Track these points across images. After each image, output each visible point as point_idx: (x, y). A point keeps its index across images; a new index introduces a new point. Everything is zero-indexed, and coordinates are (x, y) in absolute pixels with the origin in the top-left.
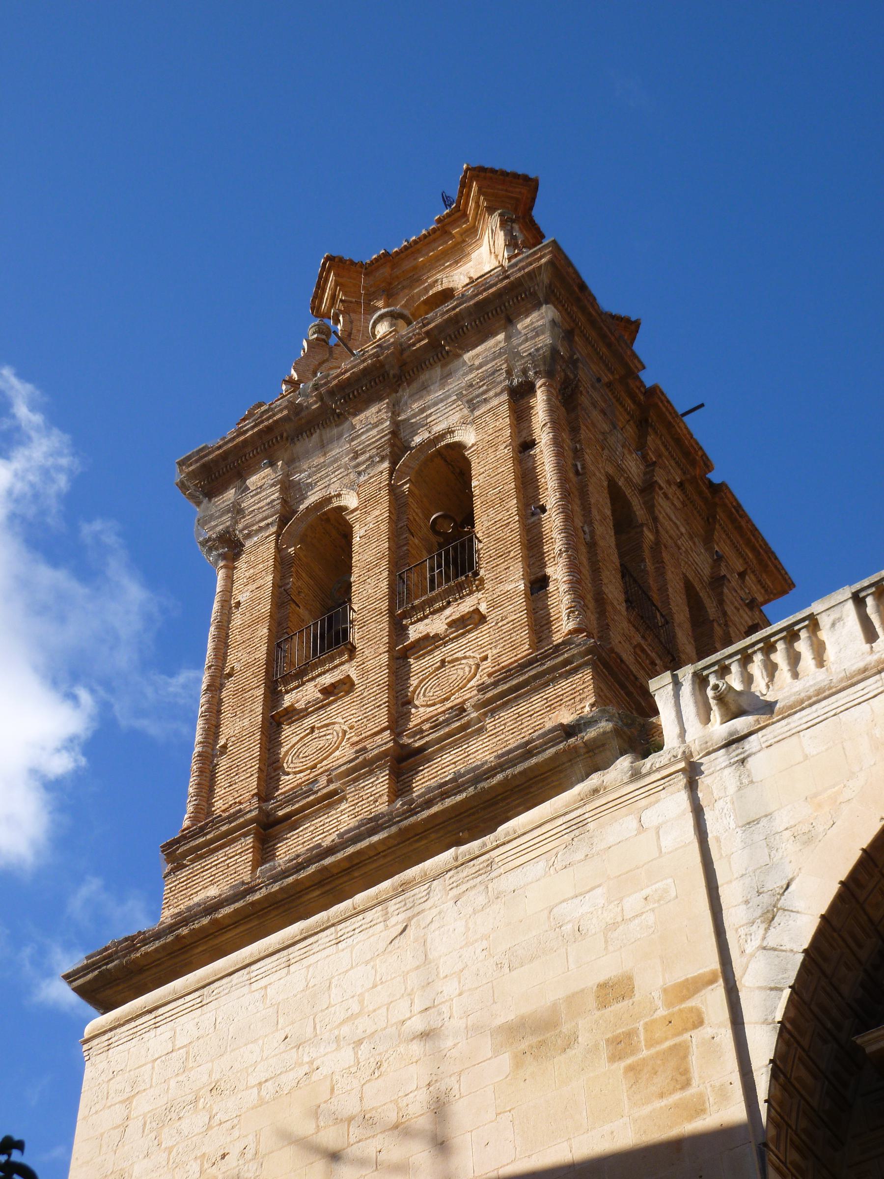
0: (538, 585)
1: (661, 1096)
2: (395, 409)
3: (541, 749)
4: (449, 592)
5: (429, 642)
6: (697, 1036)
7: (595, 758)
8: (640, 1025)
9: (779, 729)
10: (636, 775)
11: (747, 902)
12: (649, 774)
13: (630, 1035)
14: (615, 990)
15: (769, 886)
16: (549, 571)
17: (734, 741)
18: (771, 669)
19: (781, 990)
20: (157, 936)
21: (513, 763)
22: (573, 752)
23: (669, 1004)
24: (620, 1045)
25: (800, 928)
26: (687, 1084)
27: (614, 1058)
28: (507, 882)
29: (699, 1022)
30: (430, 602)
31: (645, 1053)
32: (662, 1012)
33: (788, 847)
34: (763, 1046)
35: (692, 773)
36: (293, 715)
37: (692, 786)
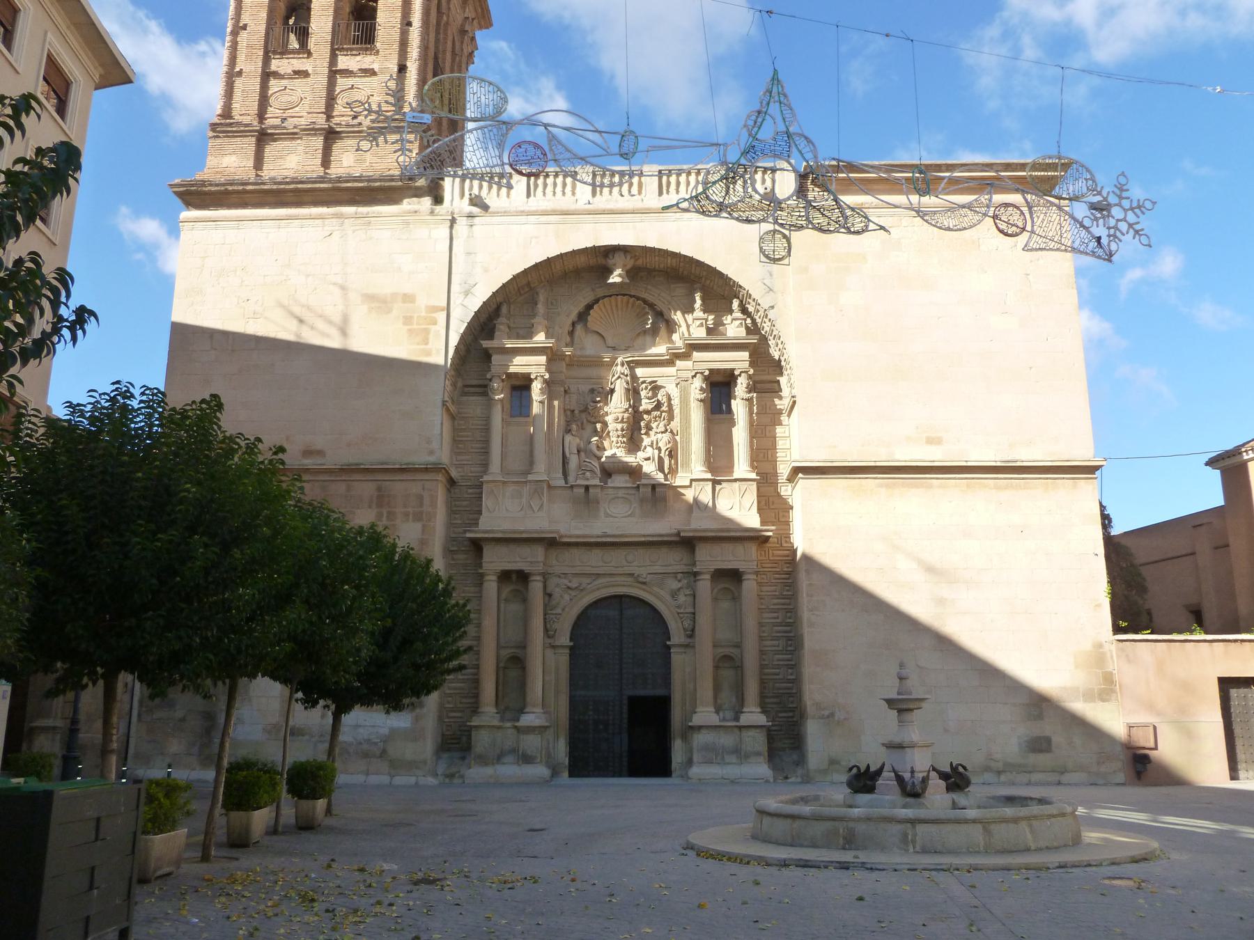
0: (402, 69)
4: (361, 49)
5: (347, 73)
6: (433, 328)
7: (418, 193)
9: (487, 219)
10: (432, 212)
13: (411, 317)
14: (408, 298)
16: (409, 64)
20: (217, 185)
24: (408, 320)
25: (475, 303)
26: (427, 344)
27: (405, 324)
29: (435, 323)
30: (351, 50)
31: (415, 327)
32: (423, 314)
34: (454, 340)
35: (453, 221)
36: (276, 75)
37: (451, 227)
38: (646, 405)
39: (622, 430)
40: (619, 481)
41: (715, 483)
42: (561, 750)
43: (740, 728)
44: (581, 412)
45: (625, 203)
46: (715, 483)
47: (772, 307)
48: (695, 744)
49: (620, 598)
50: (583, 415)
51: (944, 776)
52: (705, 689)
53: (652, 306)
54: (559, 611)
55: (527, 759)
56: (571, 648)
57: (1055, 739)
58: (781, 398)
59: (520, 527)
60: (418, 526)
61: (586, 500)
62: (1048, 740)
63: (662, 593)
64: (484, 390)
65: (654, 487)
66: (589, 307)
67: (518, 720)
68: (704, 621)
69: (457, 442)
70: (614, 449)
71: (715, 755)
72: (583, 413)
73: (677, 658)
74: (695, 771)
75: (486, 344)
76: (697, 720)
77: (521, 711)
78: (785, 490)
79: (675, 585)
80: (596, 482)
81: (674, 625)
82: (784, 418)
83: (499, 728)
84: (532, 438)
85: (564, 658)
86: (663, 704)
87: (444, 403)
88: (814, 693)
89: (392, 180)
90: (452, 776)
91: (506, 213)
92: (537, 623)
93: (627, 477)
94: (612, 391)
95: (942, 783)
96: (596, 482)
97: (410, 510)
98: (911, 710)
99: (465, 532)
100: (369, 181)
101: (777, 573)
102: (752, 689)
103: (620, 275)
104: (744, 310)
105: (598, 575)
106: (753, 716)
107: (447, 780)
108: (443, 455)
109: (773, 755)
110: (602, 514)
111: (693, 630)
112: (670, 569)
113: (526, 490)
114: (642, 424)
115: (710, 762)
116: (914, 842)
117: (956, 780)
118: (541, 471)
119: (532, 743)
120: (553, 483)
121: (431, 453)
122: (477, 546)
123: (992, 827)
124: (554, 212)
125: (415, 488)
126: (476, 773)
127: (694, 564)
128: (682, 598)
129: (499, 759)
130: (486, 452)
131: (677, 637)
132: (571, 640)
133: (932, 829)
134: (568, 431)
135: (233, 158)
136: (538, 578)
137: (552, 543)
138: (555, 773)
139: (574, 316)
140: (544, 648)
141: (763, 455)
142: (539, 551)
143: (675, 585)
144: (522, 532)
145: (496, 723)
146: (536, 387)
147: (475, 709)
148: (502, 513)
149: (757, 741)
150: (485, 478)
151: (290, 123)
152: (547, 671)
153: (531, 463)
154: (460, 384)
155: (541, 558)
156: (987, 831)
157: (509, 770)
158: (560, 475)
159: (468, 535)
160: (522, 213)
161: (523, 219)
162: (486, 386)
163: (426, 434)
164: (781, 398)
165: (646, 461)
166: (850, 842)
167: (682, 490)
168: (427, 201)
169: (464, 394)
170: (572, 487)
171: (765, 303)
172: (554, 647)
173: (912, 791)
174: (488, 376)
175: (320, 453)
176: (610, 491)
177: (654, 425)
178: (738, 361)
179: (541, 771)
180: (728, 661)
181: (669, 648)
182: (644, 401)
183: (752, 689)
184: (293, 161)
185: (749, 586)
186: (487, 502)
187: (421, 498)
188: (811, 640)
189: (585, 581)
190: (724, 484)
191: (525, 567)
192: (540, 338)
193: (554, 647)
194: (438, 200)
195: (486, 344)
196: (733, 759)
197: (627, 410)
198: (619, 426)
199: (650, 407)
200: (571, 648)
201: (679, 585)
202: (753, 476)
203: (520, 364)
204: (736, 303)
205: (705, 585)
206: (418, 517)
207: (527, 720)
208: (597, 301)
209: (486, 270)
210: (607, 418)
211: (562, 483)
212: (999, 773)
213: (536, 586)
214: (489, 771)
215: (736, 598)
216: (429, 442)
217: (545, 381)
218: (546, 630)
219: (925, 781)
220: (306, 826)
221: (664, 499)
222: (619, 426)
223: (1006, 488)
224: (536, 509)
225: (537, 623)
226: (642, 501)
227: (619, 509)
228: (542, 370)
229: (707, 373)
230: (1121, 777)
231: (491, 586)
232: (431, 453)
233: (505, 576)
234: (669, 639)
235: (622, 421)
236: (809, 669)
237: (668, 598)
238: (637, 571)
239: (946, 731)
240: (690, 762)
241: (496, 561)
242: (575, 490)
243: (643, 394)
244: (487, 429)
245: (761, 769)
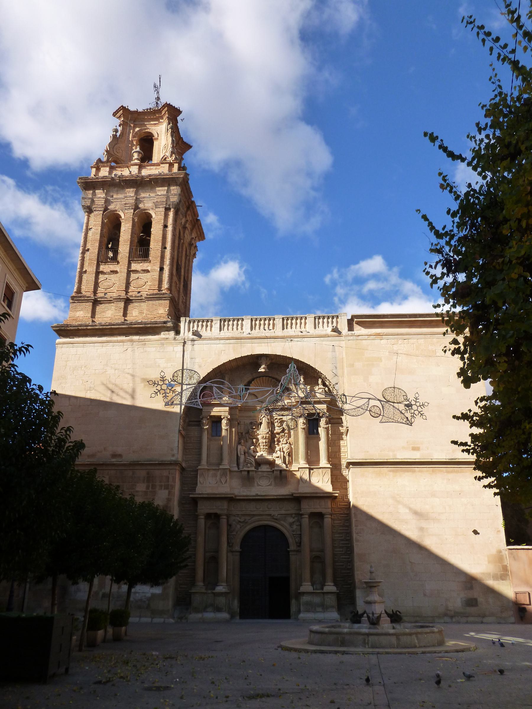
0: (162, 269)
2: (136, 193)
3: (159, 324)
4: (143, 260)
5: (136, 271)
7: (168, 329)
9: (200, 342)
10: (175, 339)
16: (165, 267)
17: (193, 340)
18: (202, 326)
20: (74, 327)
21: (153, 324)
22: (164, 327)
28: (148, 349)
30: (138, 260)
35: (185, 343)
36: (102, 273)
37: (184, 346)
38: (277, 430)
39: (266, 443)
40: (265, 468)
41: (310, 469)
42: (236, 604)
43: (324, 593)
44: (246, 433)
45: (268, 333)
46: (310, 469)
47: (337, 384)
48: (301, 601)
49: (266, 527)
50: (247, 435)
51: (389, 615)
52: (307, 574)
54: (234, 533)
55: (218, 610)
56: (241, 552)
57: (481, 599)
58: (342, 427)
59: (216, 492)
60: (167, 492)
61: (248, 479)
62: (476, 600)
63: (285, 524)
64: (199, 424)
65: (281, 471)
67: (214, 589)
68: (306, 539)
69: (185, 450)
70: (262, 452)
71: (311, 607)
72: (247, 435)
73: (293, 558)
74: (302, 615)
76: (302, 589)
77: (216, 584)
78: (345, 472)
79: (291, 520)
80: (253, 469)
81: (290, 540)
82: (344, 436)
83: (204, 593)
84: (221, 447)
85: (237, 558)
86: (287, 580)
87: (179, 431)
88: (361, 574)
89: (156, 324)
90: (181, 618)
91: (210, 339)
92: (224, 539)
93: (268, 466)
94: (261, 423)
95: (389, 619)
96: (253, 469)
97: (163, 484)
98: (375, 587)
99: (189, 494)
100: (145, 324)
101: (341, 514)
102: (329, 572)
103: (264, 368)
104: (324, 384)
105: (254, 515)
106: (330, 587)
107: (179, 620)
108: (179, 456)
109: (340, 609)
110: (256, 484)
111: (300, 543)
112: (289, 512)
113: (219, 473)
114: (276, 439)
115: (308, 611)
116: (368, 644)
117: (395, 618)
118: (226, 464)
119: (222, 601)
120: (232, 469)
121: (173, 455)
122: (195, 501)
123: (400, 637)
125: (165, 473)
126: (194, 616)
127: (300, 510)
128: (295, 527)
129: (205, 610)
130: (200, 454)
131: (292, 547)
132: (241, 548)
133: (376, 638)
134: (239, 443)
135: (81, 312)
136: (225, 517)
137: (231, 500)
138: (232, 616)
140: (227, 552)
141: (334, 456)
142: (225, 505)
143: (291, 520)
144: (216, 494)
145: (203, 590)
146: (224, 422)
147: (193, 583)
148: (208, 485)
149: (331, 600)
150: (199, 467)
151: (108, 296)
152: (228, 563)
153: (221, 459)
154: (187, 421)
156: (398, 639)
157: (210, 615)
158: (236, 465)
159: (191, 496)
160: (217, 339)
161: (218, 341)
162: (200, 421)
163: (171, 447)
164: (342, 427)
165: (277, 458)
166: (343, 643)
167: (294, 472)
168: (172, 333)
169: (189, 425)
170: (241, 471)
171: (333, 382)
172: (232, 552)
173: (374, 622)
174: (201, 417)
175: (120, 456)
176: (260, 473)
177: (281, 440)
179: (225, 615)
180: (317, 559)
181: (289, 552)
182: (276, 428)
183: (329, 572)
184: (109, 314)
185: (328, 520)
186: (200, 479)
187: (168, 478)
188: (357, 549)
189: (247, 518)
190: (315, 470)
191: (218, 512)
192: (226, 399)
193: (232, 552)
194: (178, 332)
196: (320, 609)
197: (268, 433)
198: (264, 441)
199: (279, 431)
200: (241, 552)
201: (294, 520)
202: (329, 466)
203: (216, 411)
204: (320, 381)
205: (305, 520)
206: (167, 487)
207: (220, 589)
208: (253, 380)
210: (258, 437)
211: (236, 469)
212: (452, 617)
213: (224, 521)
214: (200, 615)
215: (321, 526)
216: (172, 450)
217: (228, 419)
218: (228, 543)
219: (379, 617)
220: (117, 639)
221: (286, 477)
222: (264, 441)
223: (452, 472)
225: (224, 539)
226: (275, 478)
227: (264, 482)
228: (227, 414)
230: (512, 619)
231: (202, 522)
232: (173, 455)
233: (208, 516)
234: (289, 548)
235: (266, 438)
236: (357, 563)
237: (288, 527)
238: (273, 513)
239: (425, 595)
240: (299, 612)
241: (204, 508)
242: (243, 473)
243: (276, 424)
244: (200, 442)
245: (334, 615)
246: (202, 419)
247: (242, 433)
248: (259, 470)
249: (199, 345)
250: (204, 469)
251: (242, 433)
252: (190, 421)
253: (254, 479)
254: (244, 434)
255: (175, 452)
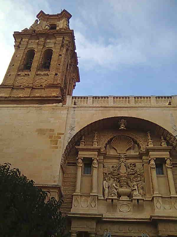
1: (53, 144)
8: (54, 136)
11: (70, 127)
12: (64, 107)
15: (73, 126)
19: (70, 138)
23: (58, 135)
24: (51, 137)
25: (74, 133)
31: (53, 139)
33: (76, 123)
50: (110, 176)
53: (133, 139)
66: (111, 139)
75: (77, 147)
80: (116, 198)
91: (85, 107)
96: (116, 198)
104: (165, 139)
113: (89, 199)
118: (95, 192)
124: (102, 107)
130: (75, 186)
137: (99, 220)
139: (106, 142)
142: (93, 225)
154: (67, 162)
155: (95, 227)
158: (102, 195)
174: (77, 158)
176: (121, 202)
178: (165, 155)
191: (88, 230)
195: (77, 147)
209: (78, 123)
211: (103, 198)
224: (93, 207)
226: (134, 205)
227: (125, 209)
229: (155, 159)
232: (55, 182)
246: (78, 159)
247: (106, 174)
248: (120, 199)
249: (78, 112)
250: (77, 195)
251: (106, 174)
252: (68, 163)
253: (117, 206)
254: (107, 174)
255: (57, 179)
